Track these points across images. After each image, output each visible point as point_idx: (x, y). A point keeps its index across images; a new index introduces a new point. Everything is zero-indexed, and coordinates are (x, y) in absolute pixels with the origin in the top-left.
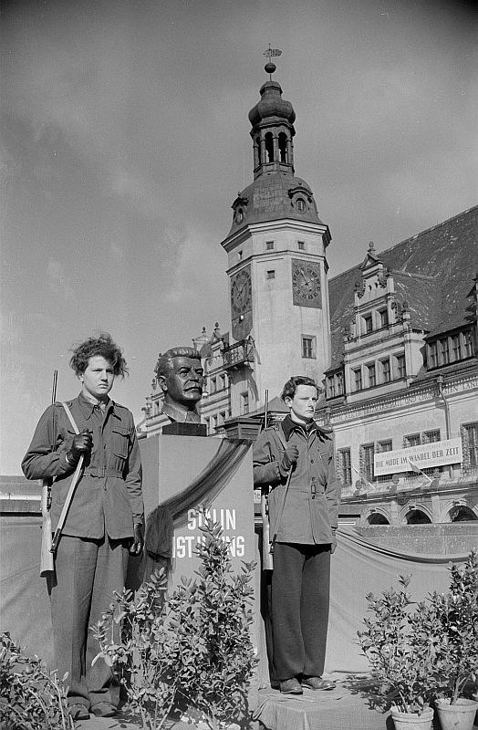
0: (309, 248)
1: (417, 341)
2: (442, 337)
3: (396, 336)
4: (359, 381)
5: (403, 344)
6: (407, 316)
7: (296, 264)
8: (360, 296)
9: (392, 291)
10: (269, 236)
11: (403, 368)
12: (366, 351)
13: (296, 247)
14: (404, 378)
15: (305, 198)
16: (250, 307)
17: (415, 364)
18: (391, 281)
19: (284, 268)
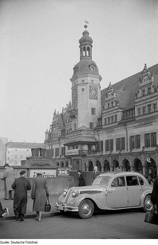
0: (95, 82)
1: (121, 112)
2: (126, 111)
3: (115, 110)
4: (106, 122)
5: (117, 112)
6: (118, 104)
7: (90, 87)
8: (107, 97)
9: (115, 97)
10: (83, 78)
11: (116, 119)
12: (108, 114)
13: (90, 82)
14: (116, 122)
15: (94, 67)
16: (77, 99)
17: (119, 119)
18: (115, 94)
19: (87, 88)
